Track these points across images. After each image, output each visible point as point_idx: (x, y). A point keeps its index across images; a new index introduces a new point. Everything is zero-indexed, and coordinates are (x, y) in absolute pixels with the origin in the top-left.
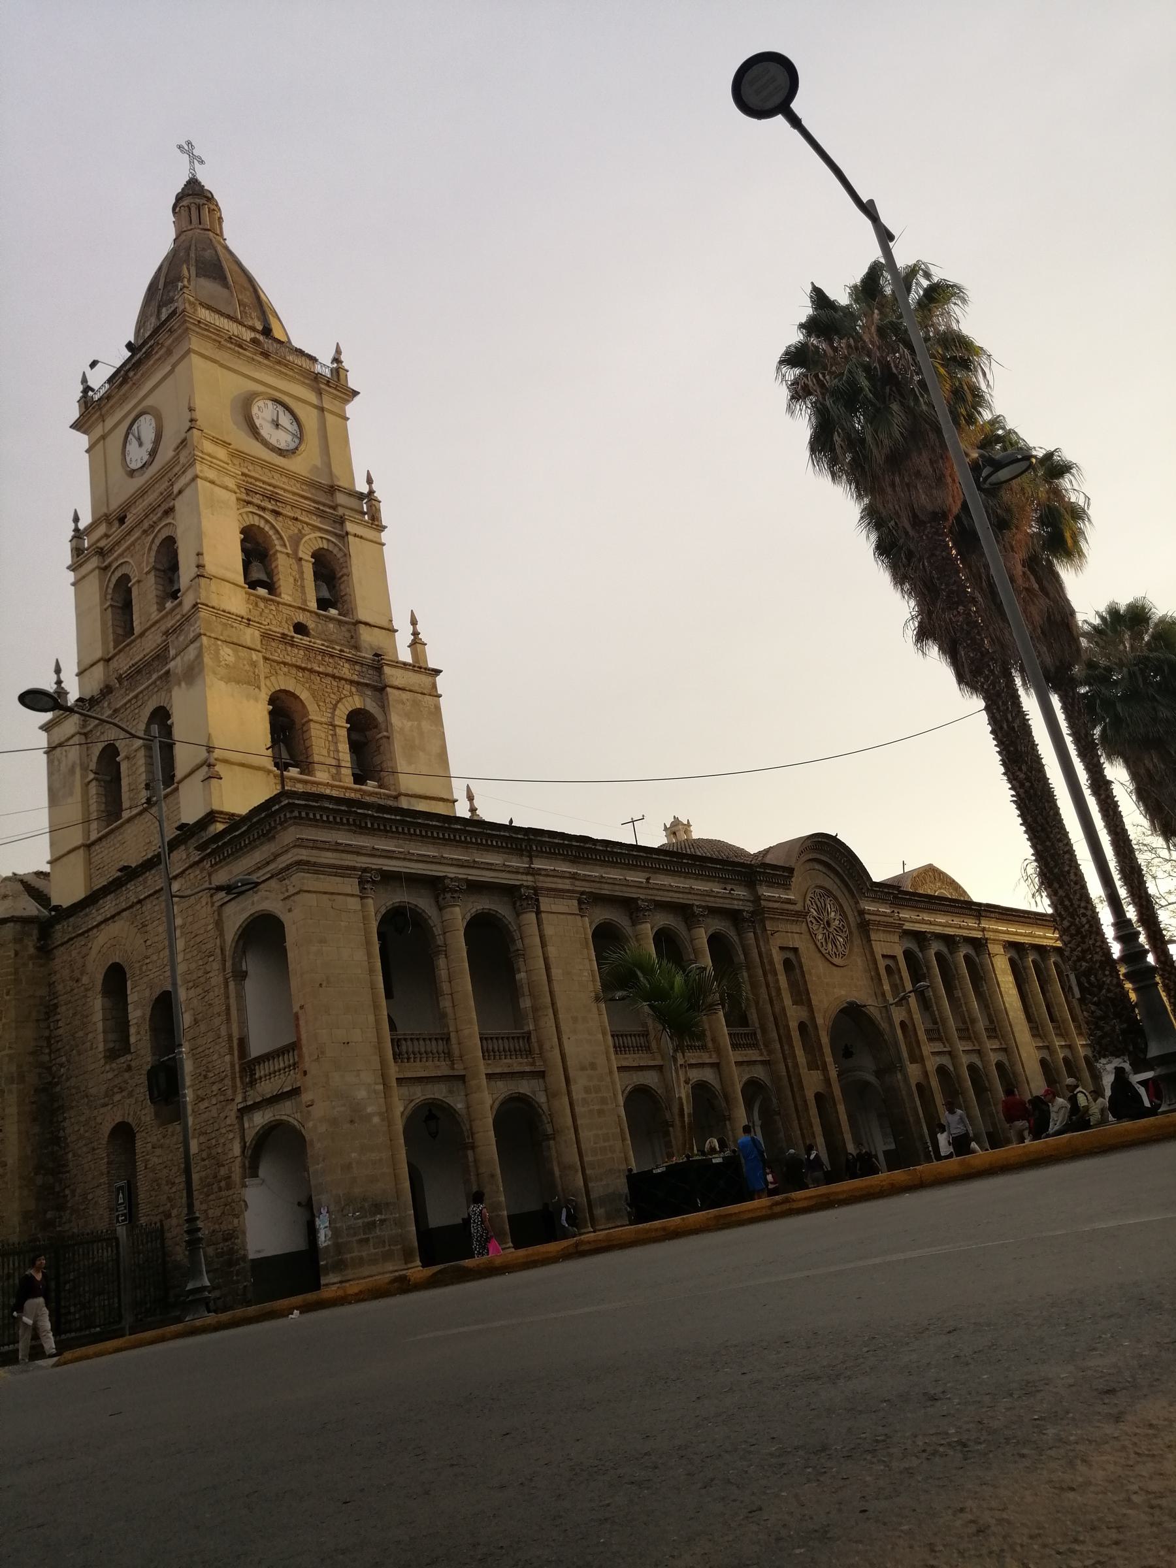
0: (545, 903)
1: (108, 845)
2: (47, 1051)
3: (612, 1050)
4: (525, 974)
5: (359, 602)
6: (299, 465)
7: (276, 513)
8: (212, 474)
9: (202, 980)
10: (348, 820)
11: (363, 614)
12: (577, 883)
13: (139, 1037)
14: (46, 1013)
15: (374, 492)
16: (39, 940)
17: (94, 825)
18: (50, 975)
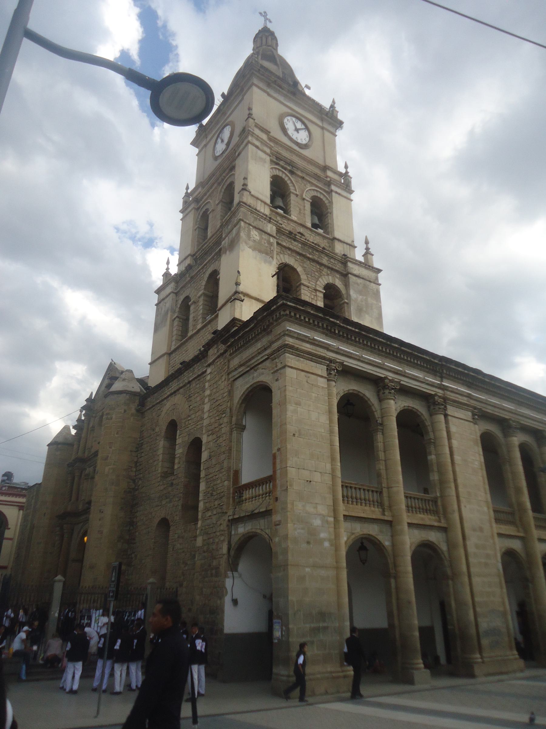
0: (451, 410)
1: (179, 353)
2: (134, 470)
3: (493, 520)
4: (434, 456)
5: (336, 227)
6: (305, 152)
7: (292, 172)
8: (257, 143)
9: (217, 429)
10: (323, 325)
11: (337, 234)
12: (472, 401)
13: (179, 465)
14: (137, 448)
15: (349, 173)
16: (138, 405)
17: (174, 343)
18: (142, 426)
